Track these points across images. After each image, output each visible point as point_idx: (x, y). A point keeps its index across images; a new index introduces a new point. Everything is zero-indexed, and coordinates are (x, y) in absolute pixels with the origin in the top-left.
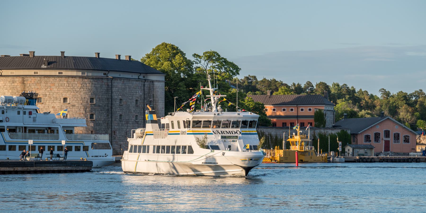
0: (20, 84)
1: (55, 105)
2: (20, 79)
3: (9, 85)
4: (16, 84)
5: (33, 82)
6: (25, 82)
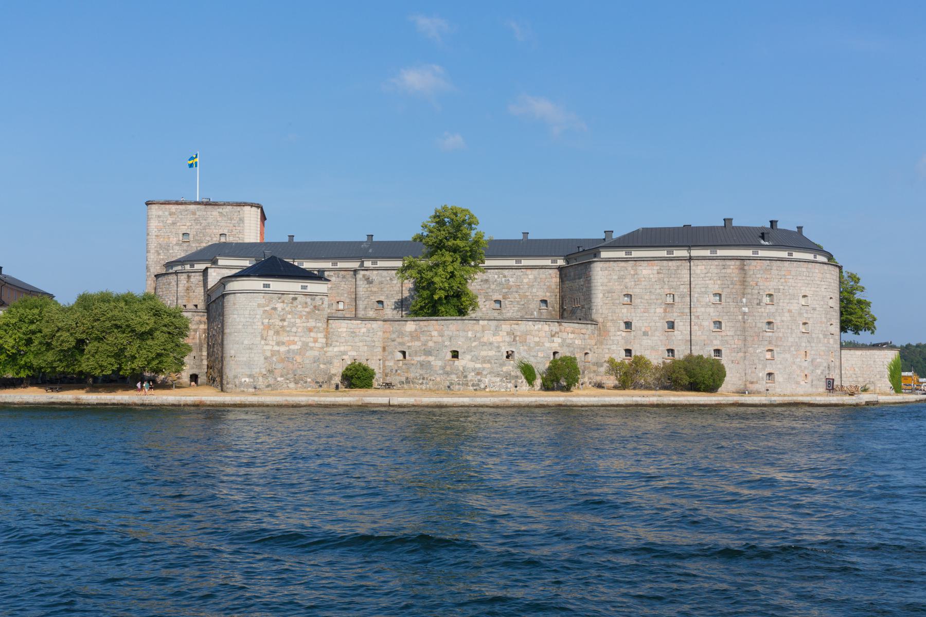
0: (737, 271)
1: (792, 308)
2: (738, 263)
3: (716, 271)
4: (729, 271)
5: (759, 268)
6: (746, 268)
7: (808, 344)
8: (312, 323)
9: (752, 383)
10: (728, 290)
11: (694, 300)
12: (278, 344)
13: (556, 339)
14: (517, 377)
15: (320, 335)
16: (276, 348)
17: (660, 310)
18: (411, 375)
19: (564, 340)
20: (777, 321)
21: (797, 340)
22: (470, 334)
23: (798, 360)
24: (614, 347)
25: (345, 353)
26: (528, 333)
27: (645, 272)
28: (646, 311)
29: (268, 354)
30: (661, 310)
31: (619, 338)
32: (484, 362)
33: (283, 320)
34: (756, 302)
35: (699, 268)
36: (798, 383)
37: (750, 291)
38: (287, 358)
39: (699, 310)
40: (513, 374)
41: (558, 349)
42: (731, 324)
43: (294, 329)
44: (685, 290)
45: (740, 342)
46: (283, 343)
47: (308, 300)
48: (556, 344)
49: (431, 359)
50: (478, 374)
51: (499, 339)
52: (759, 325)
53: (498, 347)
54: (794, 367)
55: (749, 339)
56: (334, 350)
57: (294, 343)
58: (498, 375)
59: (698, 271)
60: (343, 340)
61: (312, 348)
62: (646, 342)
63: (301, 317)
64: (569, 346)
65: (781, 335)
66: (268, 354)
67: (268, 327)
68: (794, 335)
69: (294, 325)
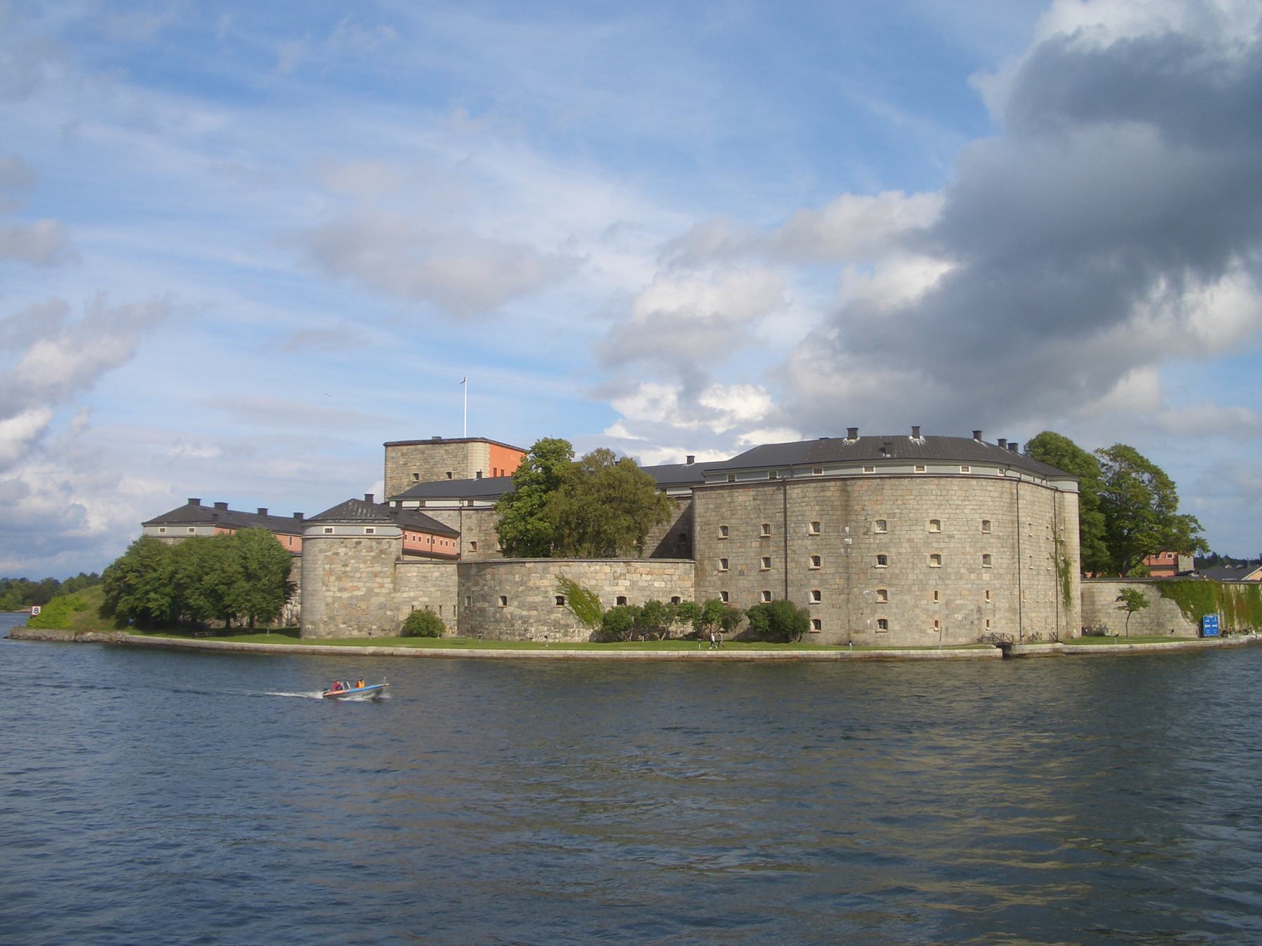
2: (839, 483)
4: (828, 494)
6: (849, 489)
7: (939, 582)
8: (377, 568)
9: (857, 632)
10: (827, 517)
11: (790, 530)
12: (340, 590)
13: (620, 582)
14: (567, 626)
15: (389, 580)
16: (338, 594)
17: (755, 544)
18: (473, 623)
19: (634, 583)
20: (891, 554)
21: (921, 577)
22: (517, 578)
23: (924, 602)
24: (711, 590)
25: (415, 598)
26: (581, 575)
27: (741, 498)
28: (743, 545)
29: (330, 600)
30: (757, 544)
31: (714, 578)
32: (530, 609)
33: (346, 565)
34: (862, 530)
35: (795, 492)
36: (923, 631)
37: (854, 517)
38: (351, 605)
39: (795, 544)
40: (562, 622)
41: (624, 594)
42: (832, 559)
43: (358, 575)
44: (782, 519)
45: (842, 582)
46: (345, 590)
47: (374, 544)
48: (622, 588)
49: (486, 605)
50: (524, 622)
51: (546, 583)
52: (867, 560)
53: (546, 592)
54: (918, 611)
55: (854, 577)
56: (399, 597)
57: (359, 589)
58: (545, 623)
59: (794, 496)
60: (413, 585)
61: (377, 594)
62: (743, 582)
63: (365, 562)
64: (643, 589)
65: (897, 571)
66: (330, 600)
67: (331, 572)
68: (917, 571)
69: (358, 570)
